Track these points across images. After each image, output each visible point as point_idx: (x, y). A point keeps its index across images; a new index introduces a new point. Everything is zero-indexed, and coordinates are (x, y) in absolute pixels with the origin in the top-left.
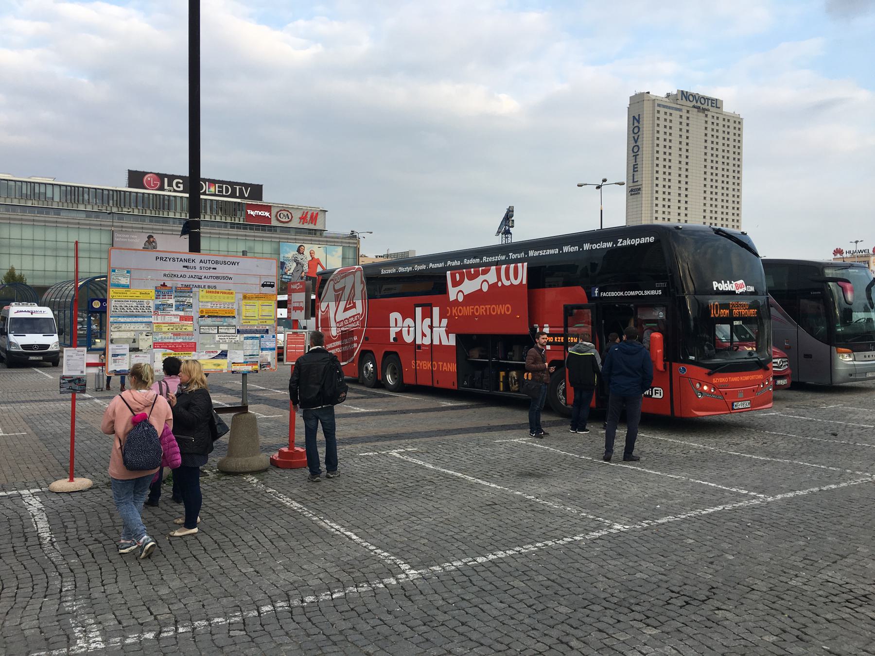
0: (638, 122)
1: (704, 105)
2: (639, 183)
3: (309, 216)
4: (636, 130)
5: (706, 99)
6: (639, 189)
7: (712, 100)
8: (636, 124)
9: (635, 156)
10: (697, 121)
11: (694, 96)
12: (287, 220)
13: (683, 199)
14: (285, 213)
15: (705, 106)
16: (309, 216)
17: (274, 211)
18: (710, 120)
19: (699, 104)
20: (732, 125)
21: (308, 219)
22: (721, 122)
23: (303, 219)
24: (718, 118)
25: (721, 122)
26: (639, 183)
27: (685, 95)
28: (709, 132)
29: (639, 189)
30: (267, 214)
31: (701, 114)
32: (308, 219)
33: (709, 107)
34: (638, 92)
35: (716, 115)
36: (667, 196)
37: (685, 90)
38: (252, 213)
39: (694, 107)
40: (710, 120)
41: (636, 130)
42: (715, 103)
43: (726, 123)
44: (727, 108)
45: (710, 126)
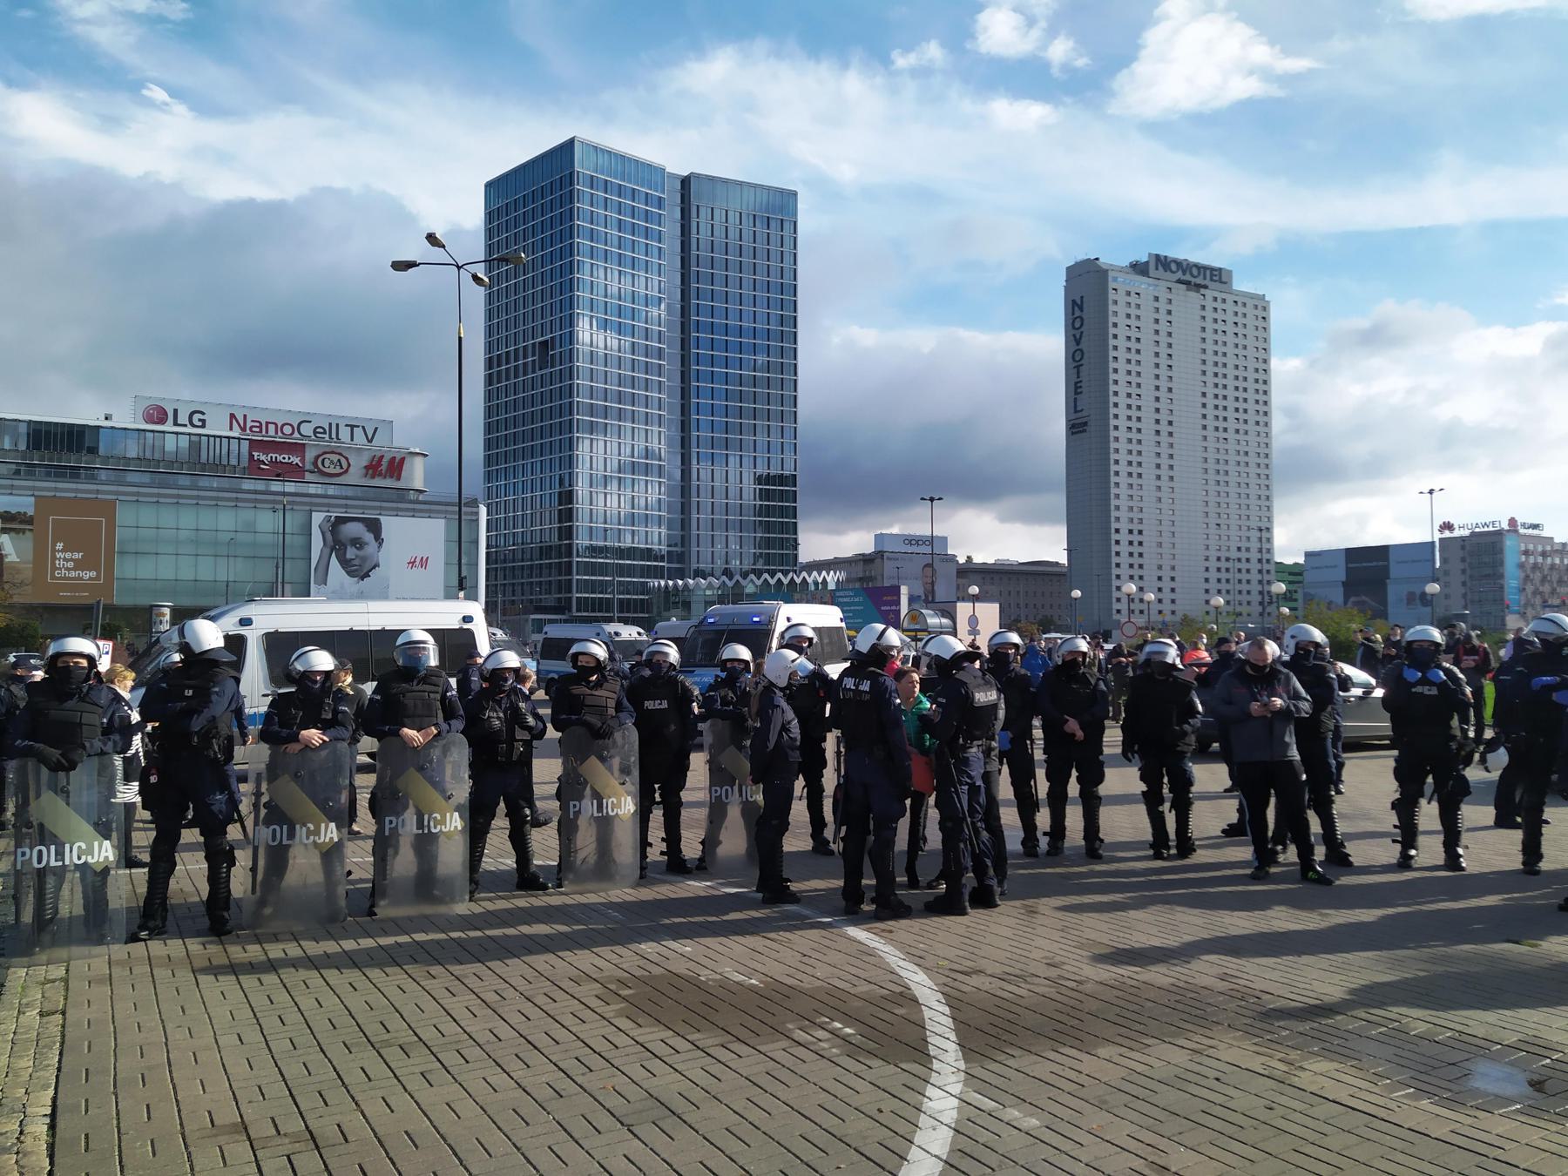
0: (1081, 309)
1: (1200, 278)
2: (1084, 414)
3: (385, 462)
4: (1077, 325)
5: (1202, 269)
6: (1085, 424)
7: (1212, 269)
8: (1078, 313)
9: (1078, 367)
10: (1187, 304)
11: (1178, 263)
12: (338, 470)
13: (1164, 438)
14: (335, 458)
15: (1199, 281)
16: (385, 462)
17: (310, 455)
18: (1210, 304)
19: (1188, 277)
20: (1249, 310)
22: (1230, 306)
23: (373, 468)
24: (1224, 301)
25: (1230, 306)
26: (1084, 414)
27: (1163, 262)
28: (1210, 326)
29: (1085, 424)
30: (296, 460)
31: (1192, 294)
33: (1207, 282)
34: (1081, 257)
35: (1220, 296)
36: (1134, 436)
37: (1163, 253)
38: (263, 458)
39: (1179, 281)
40: (1210, 304)
41: (1077, 325)
42: (1217, 276)
43: (1240, 309)
44: (1241, 284)
45: (1209, 314)
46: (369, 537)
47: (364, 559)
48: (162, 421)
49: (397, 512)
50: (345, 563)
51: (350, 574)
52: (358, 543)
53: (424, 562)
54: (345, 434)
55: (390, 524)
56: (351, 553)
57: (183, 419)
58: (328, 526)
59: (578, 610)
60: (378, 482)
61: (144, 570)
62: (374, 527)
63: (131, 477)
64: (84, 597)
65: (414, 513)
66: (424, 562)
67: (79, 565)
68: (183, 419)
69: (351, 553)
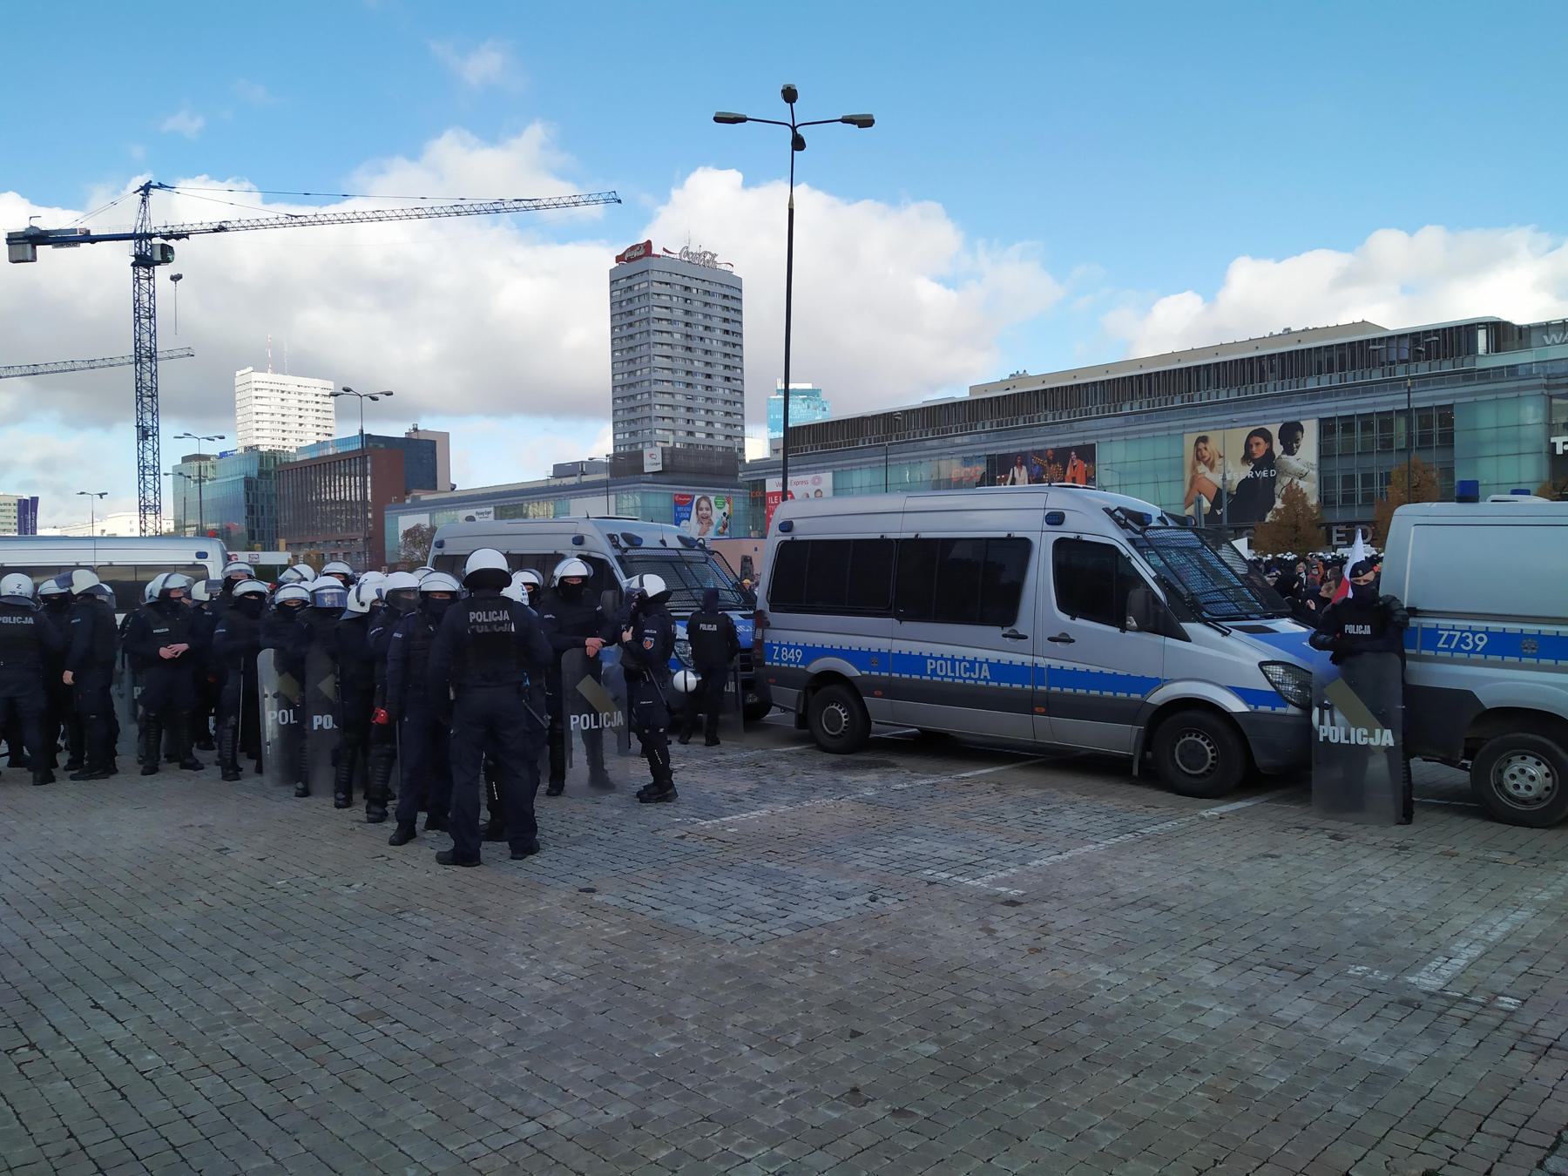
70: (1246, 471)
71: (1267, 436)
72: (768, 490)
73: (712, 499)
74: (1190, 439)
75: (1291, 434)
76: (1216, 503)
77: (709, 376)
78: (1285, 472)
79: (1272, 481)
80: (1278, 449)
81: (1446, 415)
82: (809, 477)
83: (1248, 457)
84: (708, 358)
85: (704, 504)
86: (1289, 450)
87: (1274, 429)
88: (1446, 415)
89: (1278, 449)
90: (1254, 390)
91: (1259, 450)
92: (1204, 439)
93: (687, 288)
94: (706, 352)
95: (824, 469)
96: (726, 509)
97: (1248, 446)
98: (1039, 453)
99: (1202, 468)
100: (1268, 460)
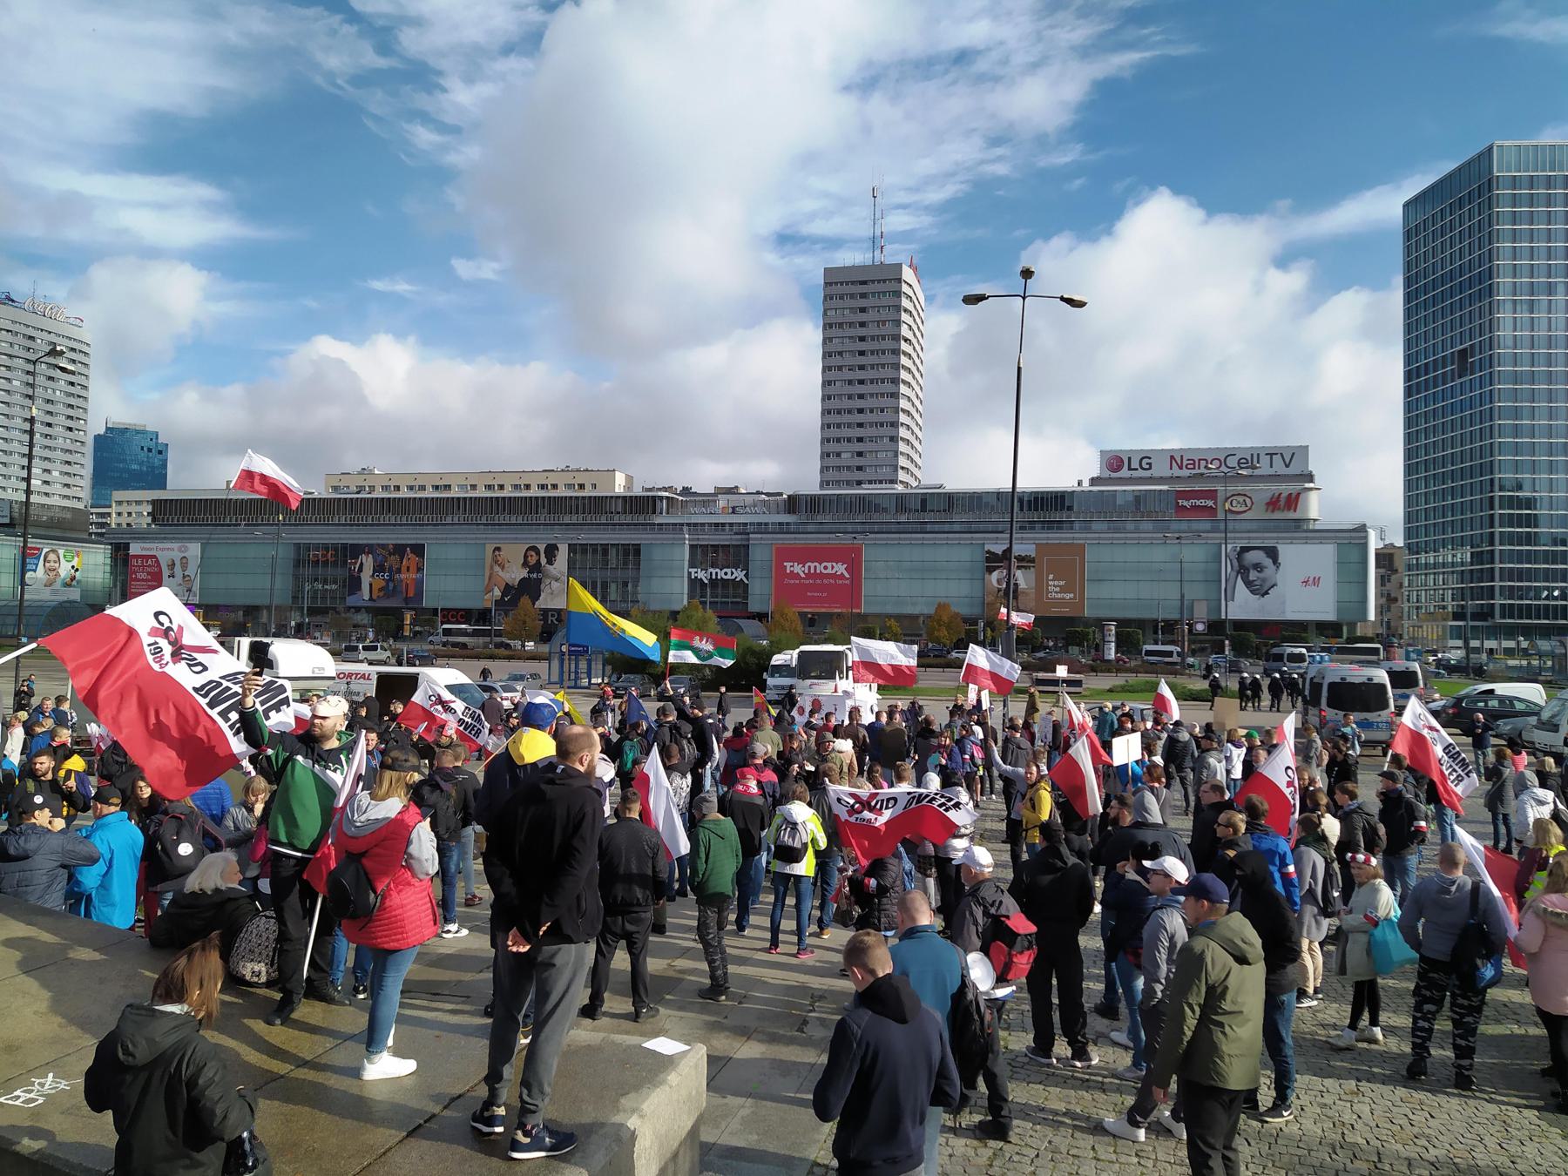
14: (1241, 499)
21: (1282, 503)
30: (1210, 503)
32: (1282, 503)
38: (1186, 503)
46: (1268, 562)
47: (1264, 580)
48: (1119, 468)
49: (1292, 541)
50: (1248, 584)
51: (1252, 592)
52: (1258, 567)
53: (1316, 581)
54: (1265, 460)
55: (1286, 552)
56: (1253, 575)
57: (1135, 464)
58: (1234, 555)
59: (1503, 617)
60: (1278, 515)
61: (1107, 591)
62: (1272, 553)
63: (1094, 526)
64: (1066, 611)
65: (1306, 541)
66: (1316, 581)
67: (1063, 590)
68: (1135, 464)
69: (1253, 575)
70: (524, 573)
71: (538, 553)
72: (132, 552)
73: (61, 552)
74: (489, 549)
75: (551, 551)
76: (504, 594)
77: (49, 425)
78: (548, 576)
79: (539, 581)
80: (543, 561)
81: (637, 549)
82: (175, 545)
83: (525, 564)
84: (49, 407)
85: (52, 557)
86: (550, 562)
87: (542, 548)
88: (637, 549)
89: (543, 561)
90: (532, 519)
91: (532, 561)
92: (498, 549)
93: (32, 338)
94: (48, 401)
95: (191, 540)
96: (75, 562)
97: (526, 556)
98: (383, 546)
99: (497, 568)
100: (537, 568)
